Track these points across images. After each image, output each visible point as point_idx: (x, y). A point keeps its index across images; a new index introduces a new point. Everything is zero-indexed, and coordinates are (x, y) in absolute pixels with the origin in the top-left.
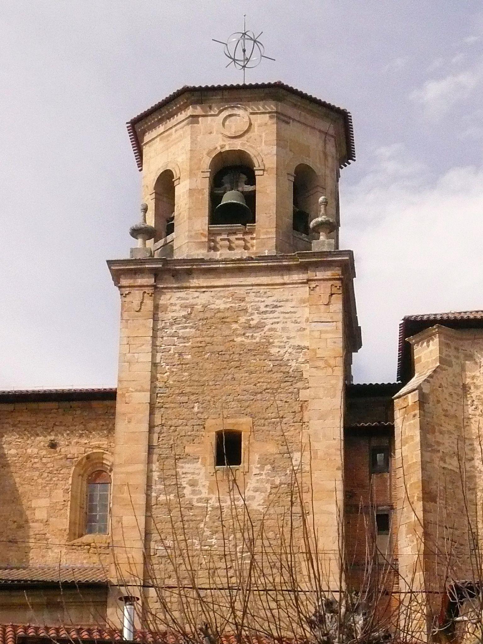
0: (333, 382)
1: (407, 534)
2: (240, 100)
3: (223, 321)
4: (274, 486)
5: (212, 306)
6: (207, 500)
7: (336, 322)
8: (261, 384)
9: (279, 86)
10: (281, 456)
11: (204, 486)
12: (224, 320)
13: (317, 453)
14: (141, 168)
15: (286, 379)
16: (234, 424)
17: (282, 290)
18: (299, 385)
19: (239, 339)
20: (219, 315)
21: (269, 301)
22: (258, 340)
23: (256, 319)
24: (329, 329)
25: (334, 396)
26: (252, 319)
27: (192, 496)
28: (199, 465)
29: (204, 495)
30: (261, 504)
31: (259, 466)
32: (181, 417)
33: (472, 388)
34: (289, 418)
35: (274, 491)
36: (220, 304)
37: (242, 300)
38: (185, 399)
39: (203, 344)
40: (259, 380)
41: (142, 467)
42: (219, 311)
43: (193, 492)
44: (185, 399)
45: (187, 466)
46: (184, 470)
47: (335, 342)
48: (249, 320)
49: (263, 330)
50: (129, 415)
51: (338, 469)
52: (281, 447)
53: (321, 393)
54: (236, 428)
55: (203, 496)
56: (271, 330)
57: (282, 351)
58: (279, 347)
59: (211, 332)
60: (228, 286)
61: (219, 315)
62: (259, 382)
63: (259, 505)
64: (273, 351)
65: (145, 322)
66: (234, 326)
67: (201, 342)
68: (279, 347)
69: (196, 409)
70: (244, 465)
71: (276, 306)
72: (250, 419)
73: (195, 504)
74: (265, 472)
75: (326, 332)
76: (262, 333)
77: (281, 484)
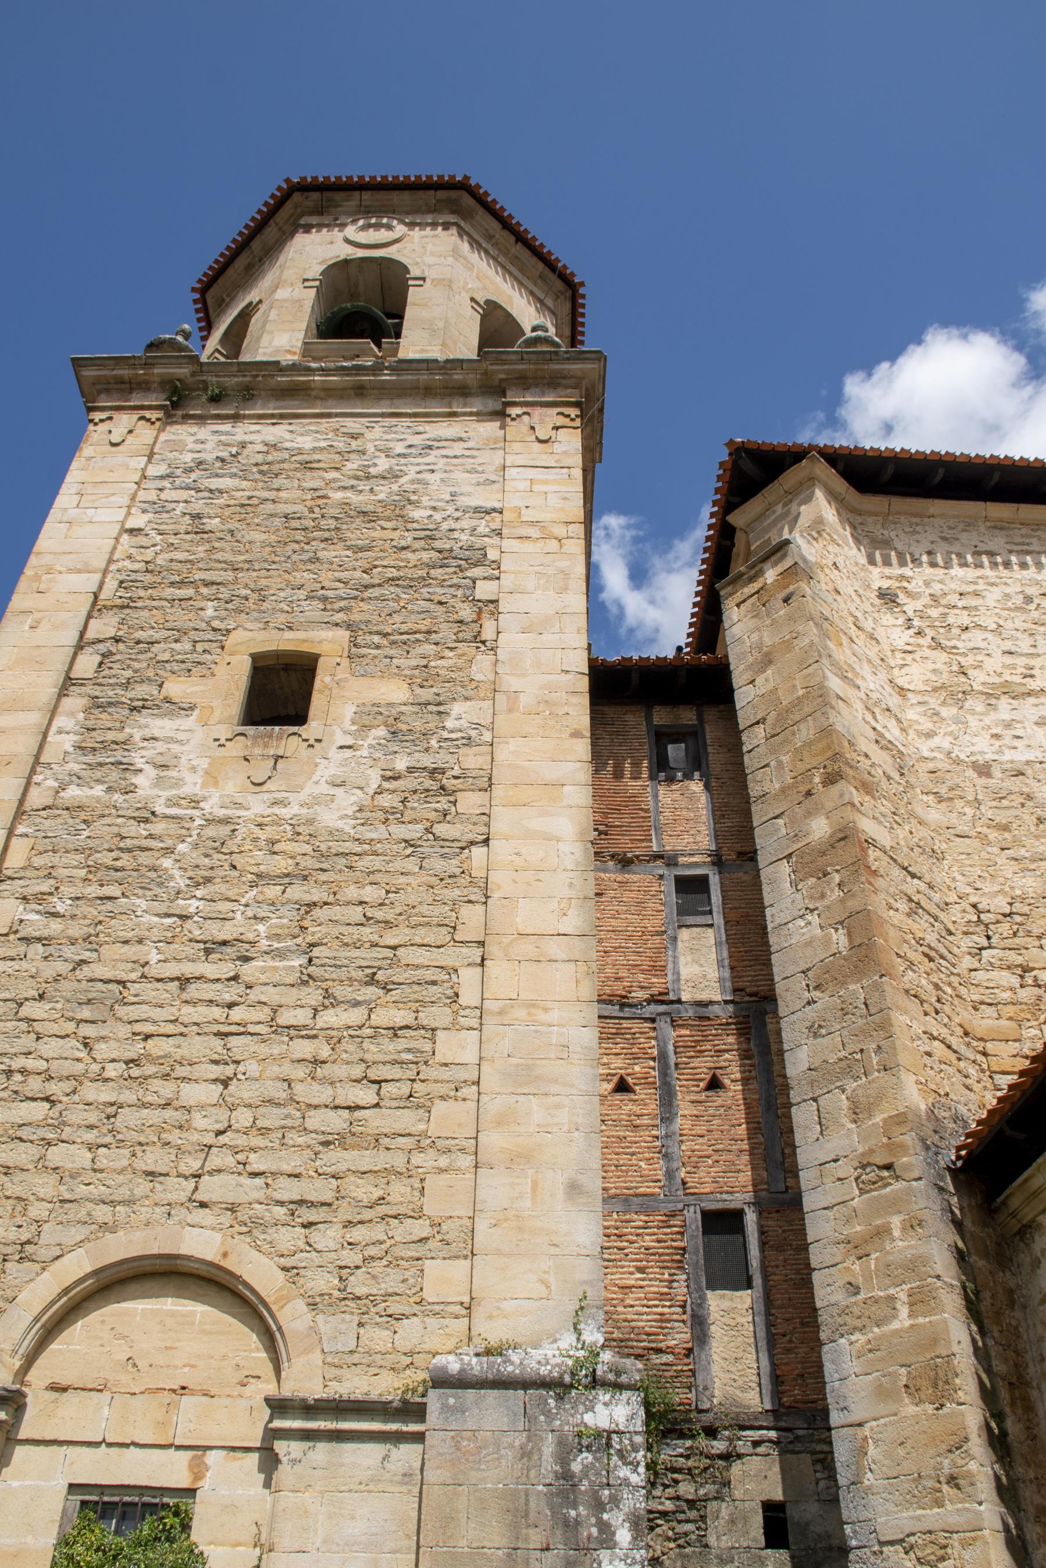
0: (563, 564)
1: (794, 884)
2: (390, 211)
3: (307, 466)
4: (389, 774)
5: (288, 445)
6: (195, 802)
7: (569, 468)
8: (380, 569)
9: (464, 186)
10: (416, 709)
11: (193, 769)
12: (309, 465)
13: (517, 698)
14: (205, 333)
15: (446, 561)
16: (305, 641)
17: (445, 424)
18: (476, 572)
19: (339, 495)
20: (299, 458)
21: (416, 440)
22: (382, 496)
23: (383, 464)
24: (551, 477)
25: (565, 589)
26: (375, 465)
27: (156, 792)
28: (189, 722)
29: (193, 785)
30: (350, 813)
31: (354, 728)
32: (168, 625)
33: (901, 596)
34: (447, 633)
35: (386, 785)
36: (306, 442)
37: (354, 436)
38: (189, 592)
39: (255, 501)
40: (376, 563)
41: (35, 718)
42: (300, 452)
43: (159, 782)
44: (189, 592)
45: (159, 722)
46: (148, 733)
47: (565, 499)
48: (369, 466)
49: (396, 482)
50: (37, 615)
51: (576, 734)
52: (418, 691)
53: (530, 583)
54: (304, 648)
55: (187, 790)
56: (412, 482)
57: (438, 516)
58: (434, 508)
59: (277, 483)
60: (329, 415)
61: (299, 458)
62: (375, 567)
63: (342, 818)
64: (417, 514)
65: (127, 459)
66: (334, 475)
67: (250, 498)
68: (434, 508)
69: (210, 612)
70: (312, 729)
71: (430, 447)
72: (344, 635)
73: (160, 809)
74: (370, 741)
75: (546, 482)
76: (395, 487)
77: (411, 770)
